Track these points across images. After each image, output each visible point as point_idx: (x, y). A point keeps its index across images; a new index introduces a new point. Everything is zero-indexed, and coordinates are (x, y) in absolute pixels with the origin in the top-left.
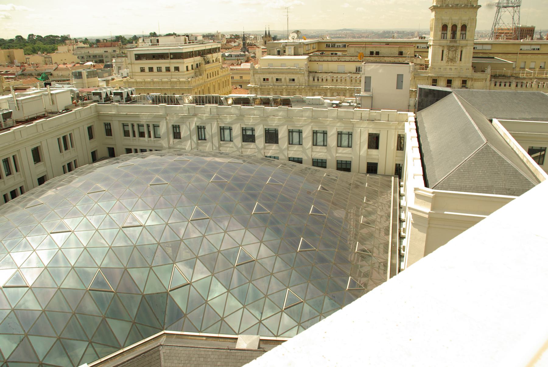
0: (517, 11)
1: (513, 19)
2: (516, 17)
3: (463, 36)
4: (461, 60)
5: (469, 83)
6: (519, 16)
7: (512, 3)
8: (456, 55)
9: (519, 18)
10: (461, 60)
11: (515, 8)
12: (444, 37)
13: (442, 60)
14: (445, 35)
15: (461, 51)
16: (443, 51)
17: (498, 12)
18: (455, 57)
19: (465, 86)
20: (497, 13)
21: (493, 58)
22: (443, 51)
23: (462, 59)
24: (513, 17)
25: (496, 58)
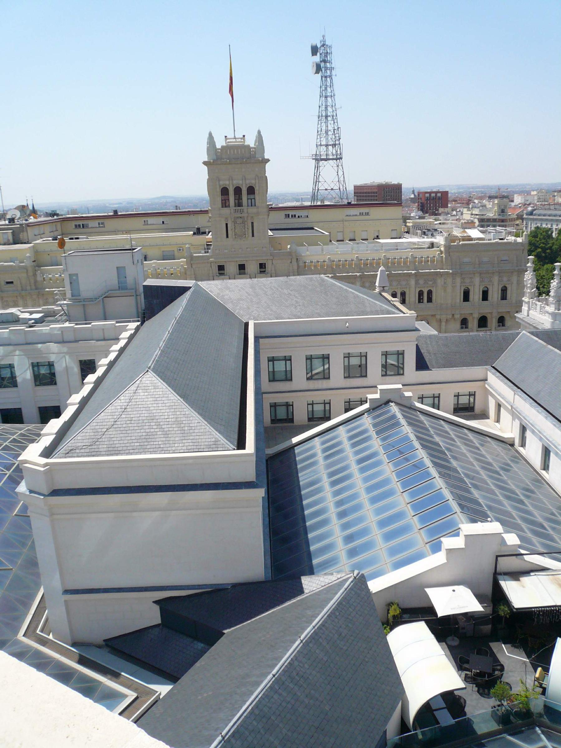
0: (340, 165)
1: (338, 175)
2: (340, 173)
3: (252, 204)
4: (253, 236)
5: (269, 267)
6: (343, 172)
7: (333, 155)
8: (246, 229)
9: (343, 174)
10: (253, 236)
11: (338, 161)
12: (225, 204)
13: (227, 237)
14: (253, 200)
15: (252, 223)
16: (227, 224)
17: (317, 167)
18: (245, 232)
19: (265, 271)
20: (316, 168)
21: (312, 229)
22: (227, 224)
23: (229, 236)
24: (337, 172)
25: (316, 230)
